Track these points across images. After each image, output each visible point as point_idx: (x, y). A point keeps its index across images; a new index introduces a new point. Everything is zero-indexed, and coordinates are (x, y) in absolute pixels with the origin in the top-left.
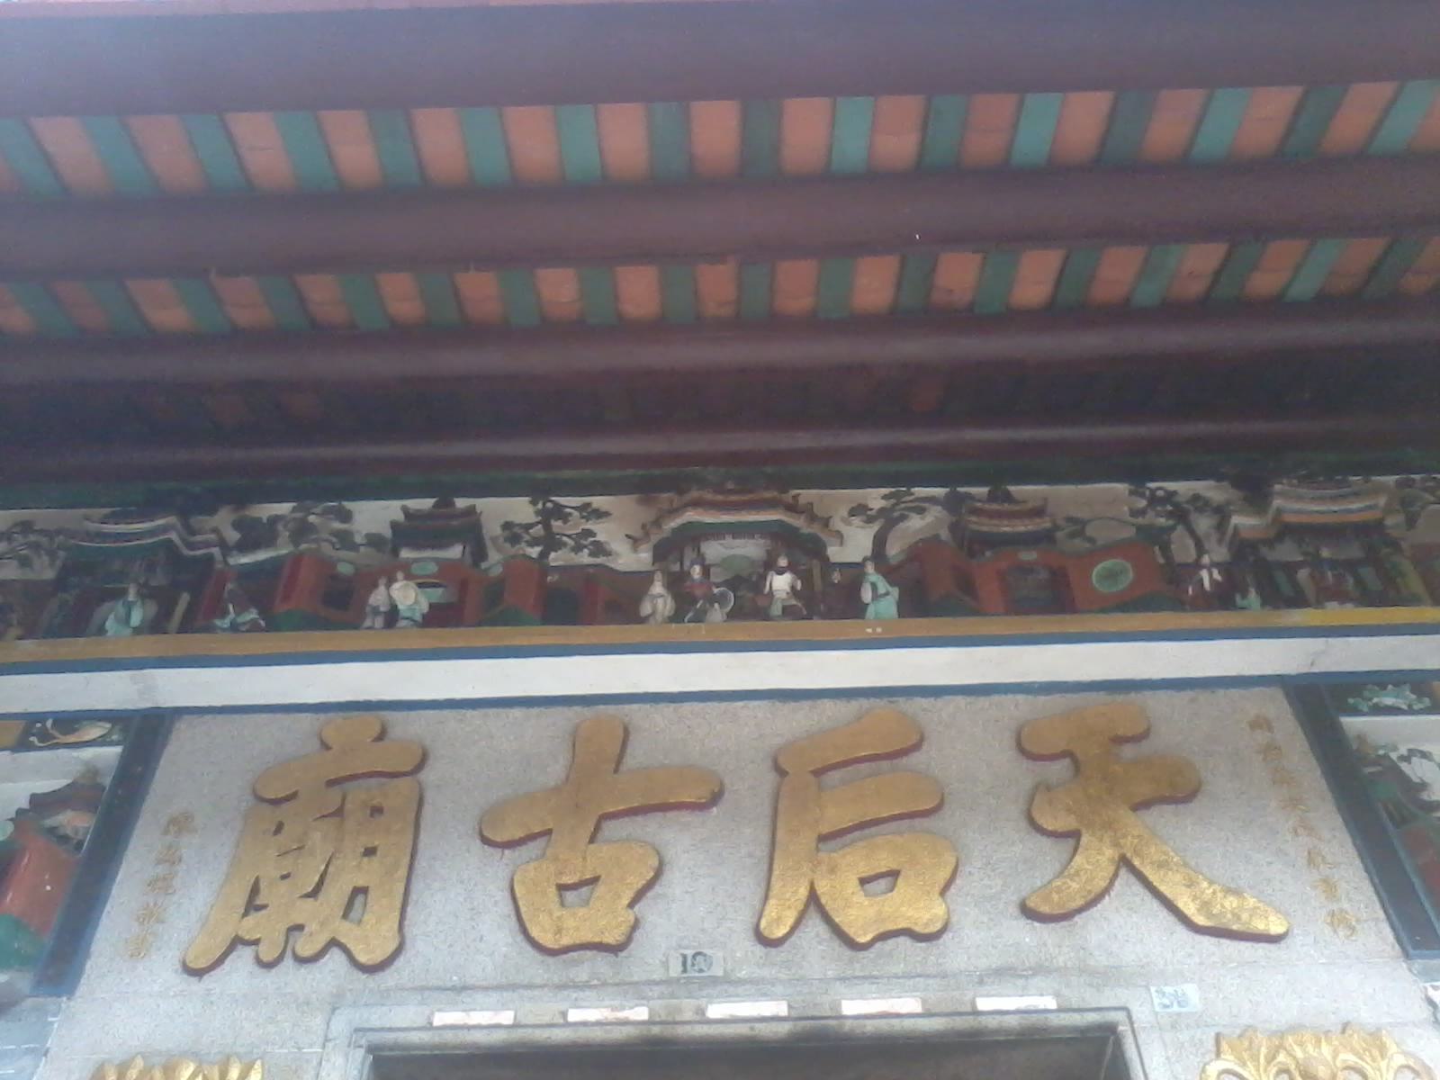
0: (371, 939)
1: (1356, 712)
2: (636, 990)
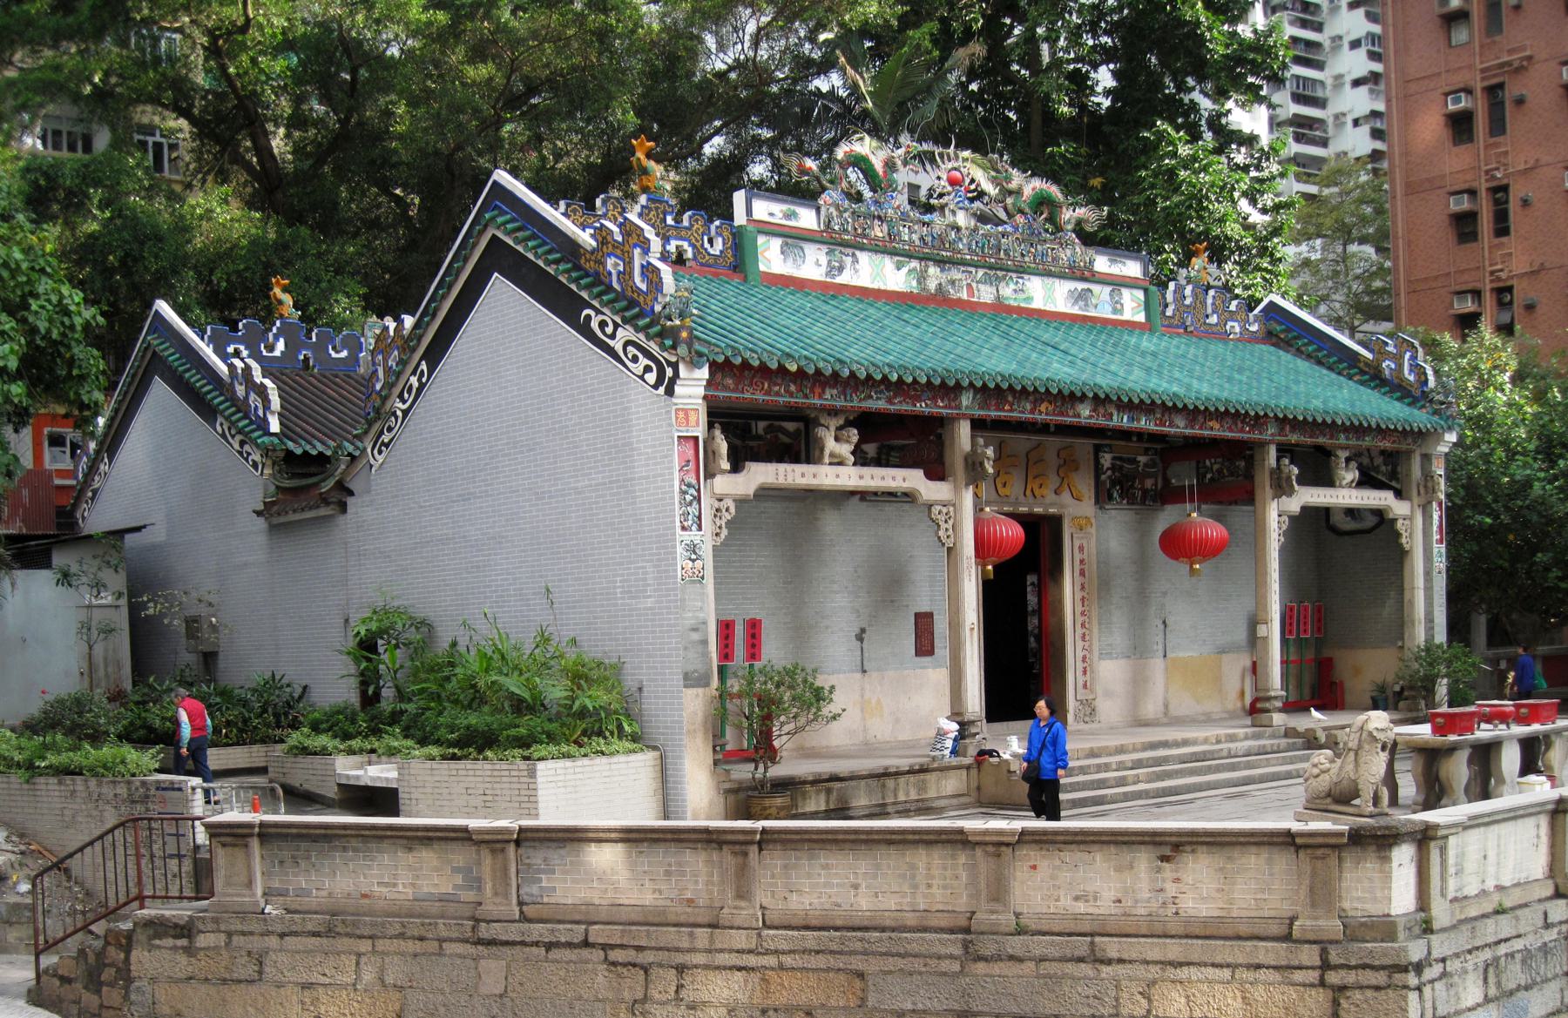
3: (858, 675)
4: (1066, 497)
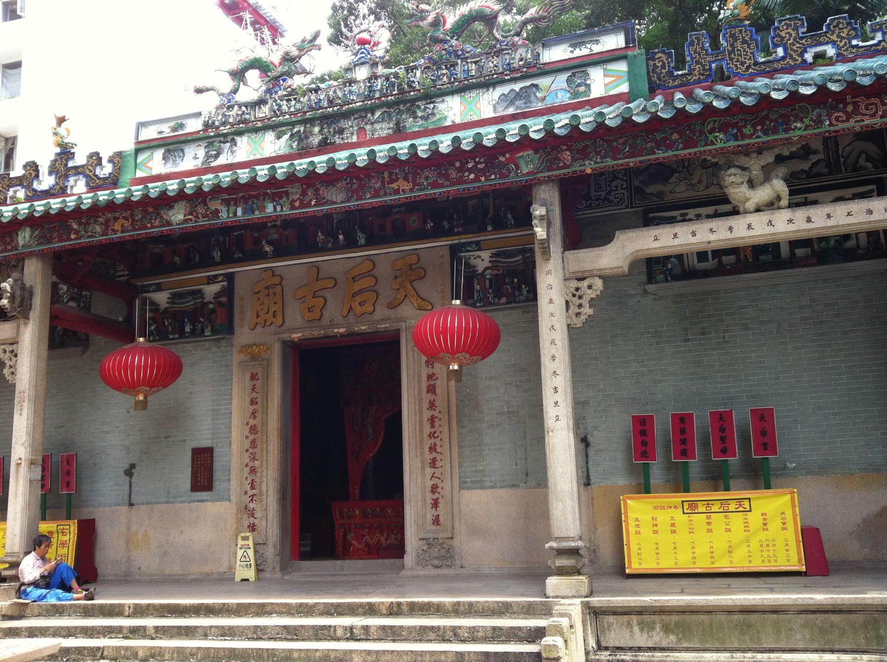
2: (322, 328)
3: (125, 509)
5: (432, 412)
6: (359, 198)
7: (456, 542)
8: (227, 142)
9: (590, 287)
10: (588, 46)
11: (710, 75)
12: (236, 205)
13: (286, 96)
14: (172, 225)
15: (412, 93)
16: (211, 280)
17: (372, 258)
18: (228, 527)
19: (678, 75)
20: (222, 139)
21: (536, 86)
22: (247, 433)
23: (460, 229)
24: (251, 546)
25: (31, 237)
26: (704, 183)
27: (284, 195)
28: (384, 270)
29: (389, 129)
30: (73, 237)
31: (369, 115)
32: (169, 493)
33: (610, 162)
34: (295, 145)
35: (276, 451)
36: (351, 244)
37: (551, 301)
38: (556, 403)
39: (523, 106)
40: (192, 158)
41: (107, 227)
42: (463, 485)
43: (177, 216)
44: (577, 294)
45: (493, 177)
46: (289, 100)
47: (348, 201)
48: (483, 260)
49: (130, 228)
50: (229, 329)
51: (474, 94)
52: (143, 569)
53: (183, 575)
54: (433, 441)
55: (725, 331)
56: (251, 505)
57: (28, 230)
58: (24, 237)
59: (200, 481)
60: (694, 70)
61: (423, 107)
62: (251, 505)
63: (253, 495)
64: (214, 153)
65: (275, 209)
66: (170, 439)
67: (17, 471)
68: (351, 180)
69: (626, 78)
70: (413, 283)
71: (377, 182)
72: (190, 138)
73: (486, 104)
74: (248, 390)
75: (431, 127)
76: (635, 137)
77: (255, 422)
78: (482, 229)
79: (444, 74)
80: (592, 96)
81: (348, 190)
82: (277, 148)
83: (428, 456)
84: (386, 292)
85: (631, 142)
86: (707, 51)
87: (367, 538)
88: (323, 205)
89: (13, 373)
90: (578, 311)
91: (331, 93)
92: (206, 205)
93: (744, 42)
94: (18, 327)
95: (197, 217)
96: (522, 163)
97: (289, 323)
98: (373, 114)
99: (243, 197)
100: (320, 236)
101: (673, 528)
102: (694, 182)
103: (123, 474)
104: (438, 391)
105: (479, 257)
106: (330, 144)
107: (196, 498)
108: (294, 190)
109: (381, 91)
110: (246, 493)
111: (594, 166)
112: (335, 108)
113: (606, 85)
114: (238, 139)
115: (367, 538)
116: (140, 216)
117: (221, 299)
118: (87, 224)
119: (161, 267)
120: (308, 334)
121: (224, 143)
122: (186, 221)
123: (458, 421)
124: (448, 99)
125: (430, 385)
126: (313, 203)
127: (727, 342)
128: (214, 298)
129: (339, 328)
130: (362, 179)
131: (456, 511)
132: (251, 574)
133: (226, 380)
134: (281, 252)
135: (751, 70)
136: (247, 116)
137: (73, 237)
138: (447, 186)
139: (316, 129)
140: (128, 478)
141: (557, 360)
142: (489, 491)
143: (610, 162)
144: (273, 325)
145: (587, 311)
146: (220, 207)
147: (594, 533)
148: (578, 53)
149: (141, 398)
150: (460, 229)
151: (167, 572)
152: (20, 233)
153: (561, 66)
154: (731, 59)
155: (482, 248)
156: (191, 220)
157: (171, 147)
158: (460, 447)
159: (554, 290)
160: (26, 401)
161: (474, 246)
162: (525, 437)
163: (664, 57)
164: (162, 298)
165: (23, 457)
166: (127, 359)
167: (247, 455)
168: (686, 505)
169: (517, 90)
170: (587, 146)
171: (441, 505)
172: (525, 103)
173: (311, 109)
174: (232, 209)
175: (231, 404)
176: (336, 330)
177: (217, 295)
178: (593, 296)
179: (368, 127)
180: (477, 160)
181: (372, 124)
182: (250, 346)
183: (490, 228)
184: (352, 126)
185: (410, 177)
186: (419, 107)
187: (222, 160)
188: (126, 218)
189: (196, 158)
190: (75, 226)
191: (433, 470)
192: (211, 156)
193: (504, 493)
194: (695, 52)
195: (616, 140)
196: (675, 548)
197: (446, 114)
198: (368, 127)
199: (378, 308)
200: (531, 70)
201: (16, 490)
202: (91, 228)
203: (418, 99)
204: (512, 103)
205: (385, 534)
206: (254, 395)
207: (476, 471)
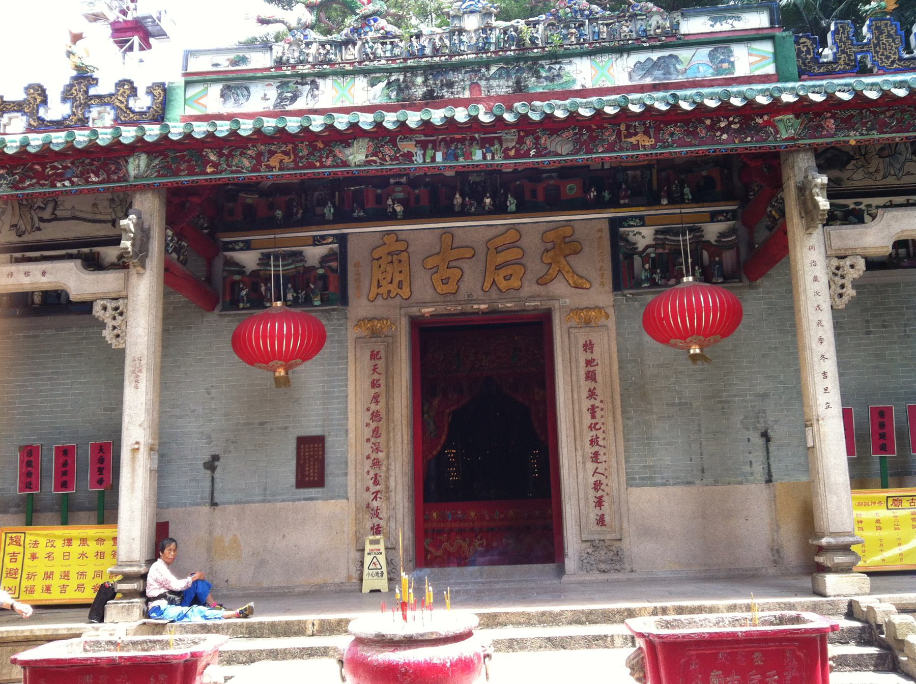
0: (405, 292)
1: (624, 227)
2: (459, 303)
3: (206, 509)
4: (559, 287)
5: (592, 402)
6: (589, 152)
7: (625, 544)
8: (306, 83)
9: (852, 266)
10: (730, 21)
11: (855, 66)
12: (435, 149)
13: (379, 38)
14: (349, 166)
15: (535, 51)
16: (317, 241)
17: (517, 227)
18: (346, 529)
19: (823, 63)
20: (299, 80)
21: (676, 57)
22: (367, 419)
23: (627, 201)
24: (383, 550)
25: (148, 166)
26: (882, 173)
27: (496, 142)
28: (532, 242)
29: (508, 87)
30: (209, 170)
31: (483, 70)
32: (265, 489)
33: (875, 135)
34: (393, 95)
35: (405, 442)
36: (500, 210)
37: (816, 279)
38: (826, 389)
39: (663, 77)
40: (260, 99)
41: (259, 163)
42: (631, 482)
43: (357, 155)
44: (840, 272)
45: (749, 139)
46: (383, 44)
47: (576, 154)
48: (644, 237)
49: (292, 165)
50: (344, 300)
51: (606, 58)
52: (233, 581)
53: (288, 588)
54: (594, 433)
55: (906, 325)
56: (375, 504)
57: (144, 157)
58: (136, 166)
59: (309, 476)
60: (840, 59)
61: (547, 67)
62: (375, 504)
63: (377, 492)
64: (289, 95)
65: (484, 157)
66: (267, 426)
67: (133, 460)
68: (581, 130)
69: (771, 60)
70: (568, 258)
71: (611, 135)
72: (259, 74)
73: (619, 71)
74: (368, 371)
75: (558, 89)
76: (903, 111)
77: (378, 407)
78: (654, 201)
79: (572, 33)
80: (736, 75)
81: (576, 141)
82: (371, 97)
83: (590, 450)
84: (535, 267)
85: (898, 116)
86: (852, 40)
87: (446, 545)
88: (544, 156)
89: (118, 336)
90: (841, 291)
91: (437, 40)
92: (395, 145)
93: (889, 36)
94: (127, 279)
95: (384, 159)
96: (781, 127)
97: (417, 296)
98: (488, 69)
99: (443, 140)
100: (458, 199)
101: (878, 525)
102: (872, 170)
103: (201, 467)
104: (599, 378)
105: (640, 233)
106: (437, 97)
107: (302, 497)
108: (508, 137)
109: (497, 44)
110: (368, 489)
111: (859, 138)
112: (443, 58)
113: (751, 64)
114: (320, 82)
115: (446, 545)
116: (305, 152)
117: (331, 264)
118: (230, 156)
119: (254, 221)
120: (441, 309)
121: (303, 84)
122: (368, 163)
123: (623, 412)
124: (577, 61)
125: (589, 372)
126: (532, 153)
127: (909, 336)
128: (320, 263)
129: (479, 304)
130: (594, 130)
131: (624, 510)
132: (382, 584)
133: (339, 358)
134: (412, 214)
135: (895, 65)
136: (333, 57)
137: (209, 170)
138: (695, 145)
139: (419, 80)
140: (209, 472)
141: (825, 343)
142: (660, 489)
143: (875, 135)
144: (398, 298)
145: (850, 292)
146: (414, 150)
147: (777, 531)
148: (718, 27)
149: (281, 372)
150: (627, 201)
151: (265, 585)
152: (131, 160)
153: (703, 38)
154: (877, 52)
155: (647, 223)
156: (375, 162)
157: (232, 83)
158: (626, 440)
159: (818, 267)
160: (144, 370)
161: (638, 221)
162: (700, 431)
163: (809, 43)
164: (249, 259)
165: (142, 441)
166: (273, 327)
167: (370, 445)
168: (890, 502)
169: (655, 59)
170: (852, 116)
171: (606, 504)
172: (664, 74)
173: (412, 55)
174: (430, 153)
175: (346, 386)
176: (475, 307)
177: (324, 260)
178: (856, 276)
179: (483, 83)
180: (731, 119)
181: (488, 79)
182: (371, 320)
183: (665, 202)
184: (463, 80)
185: (652, 131)
186: (543, 67)
187: (301, 104)
188: (285, 153)
189: (265, 98)
190: (213, 158)
191: (596, 465)
192: (286, 98)
193: (678, 491)
194: (841, 41)
195: (883, 113)
196: (881, 545)
197: (575, 76)
198: (483, 83)
199: (526, 284)
200: (669, 40)
201: (133, 483)
202: (235, 161)
203: (543, 57)
204: (648, 72)
205: (467, 539)
206: (376, 376)
207: (645, 467)
